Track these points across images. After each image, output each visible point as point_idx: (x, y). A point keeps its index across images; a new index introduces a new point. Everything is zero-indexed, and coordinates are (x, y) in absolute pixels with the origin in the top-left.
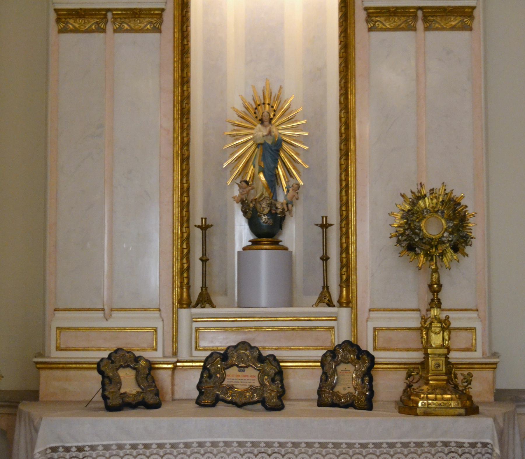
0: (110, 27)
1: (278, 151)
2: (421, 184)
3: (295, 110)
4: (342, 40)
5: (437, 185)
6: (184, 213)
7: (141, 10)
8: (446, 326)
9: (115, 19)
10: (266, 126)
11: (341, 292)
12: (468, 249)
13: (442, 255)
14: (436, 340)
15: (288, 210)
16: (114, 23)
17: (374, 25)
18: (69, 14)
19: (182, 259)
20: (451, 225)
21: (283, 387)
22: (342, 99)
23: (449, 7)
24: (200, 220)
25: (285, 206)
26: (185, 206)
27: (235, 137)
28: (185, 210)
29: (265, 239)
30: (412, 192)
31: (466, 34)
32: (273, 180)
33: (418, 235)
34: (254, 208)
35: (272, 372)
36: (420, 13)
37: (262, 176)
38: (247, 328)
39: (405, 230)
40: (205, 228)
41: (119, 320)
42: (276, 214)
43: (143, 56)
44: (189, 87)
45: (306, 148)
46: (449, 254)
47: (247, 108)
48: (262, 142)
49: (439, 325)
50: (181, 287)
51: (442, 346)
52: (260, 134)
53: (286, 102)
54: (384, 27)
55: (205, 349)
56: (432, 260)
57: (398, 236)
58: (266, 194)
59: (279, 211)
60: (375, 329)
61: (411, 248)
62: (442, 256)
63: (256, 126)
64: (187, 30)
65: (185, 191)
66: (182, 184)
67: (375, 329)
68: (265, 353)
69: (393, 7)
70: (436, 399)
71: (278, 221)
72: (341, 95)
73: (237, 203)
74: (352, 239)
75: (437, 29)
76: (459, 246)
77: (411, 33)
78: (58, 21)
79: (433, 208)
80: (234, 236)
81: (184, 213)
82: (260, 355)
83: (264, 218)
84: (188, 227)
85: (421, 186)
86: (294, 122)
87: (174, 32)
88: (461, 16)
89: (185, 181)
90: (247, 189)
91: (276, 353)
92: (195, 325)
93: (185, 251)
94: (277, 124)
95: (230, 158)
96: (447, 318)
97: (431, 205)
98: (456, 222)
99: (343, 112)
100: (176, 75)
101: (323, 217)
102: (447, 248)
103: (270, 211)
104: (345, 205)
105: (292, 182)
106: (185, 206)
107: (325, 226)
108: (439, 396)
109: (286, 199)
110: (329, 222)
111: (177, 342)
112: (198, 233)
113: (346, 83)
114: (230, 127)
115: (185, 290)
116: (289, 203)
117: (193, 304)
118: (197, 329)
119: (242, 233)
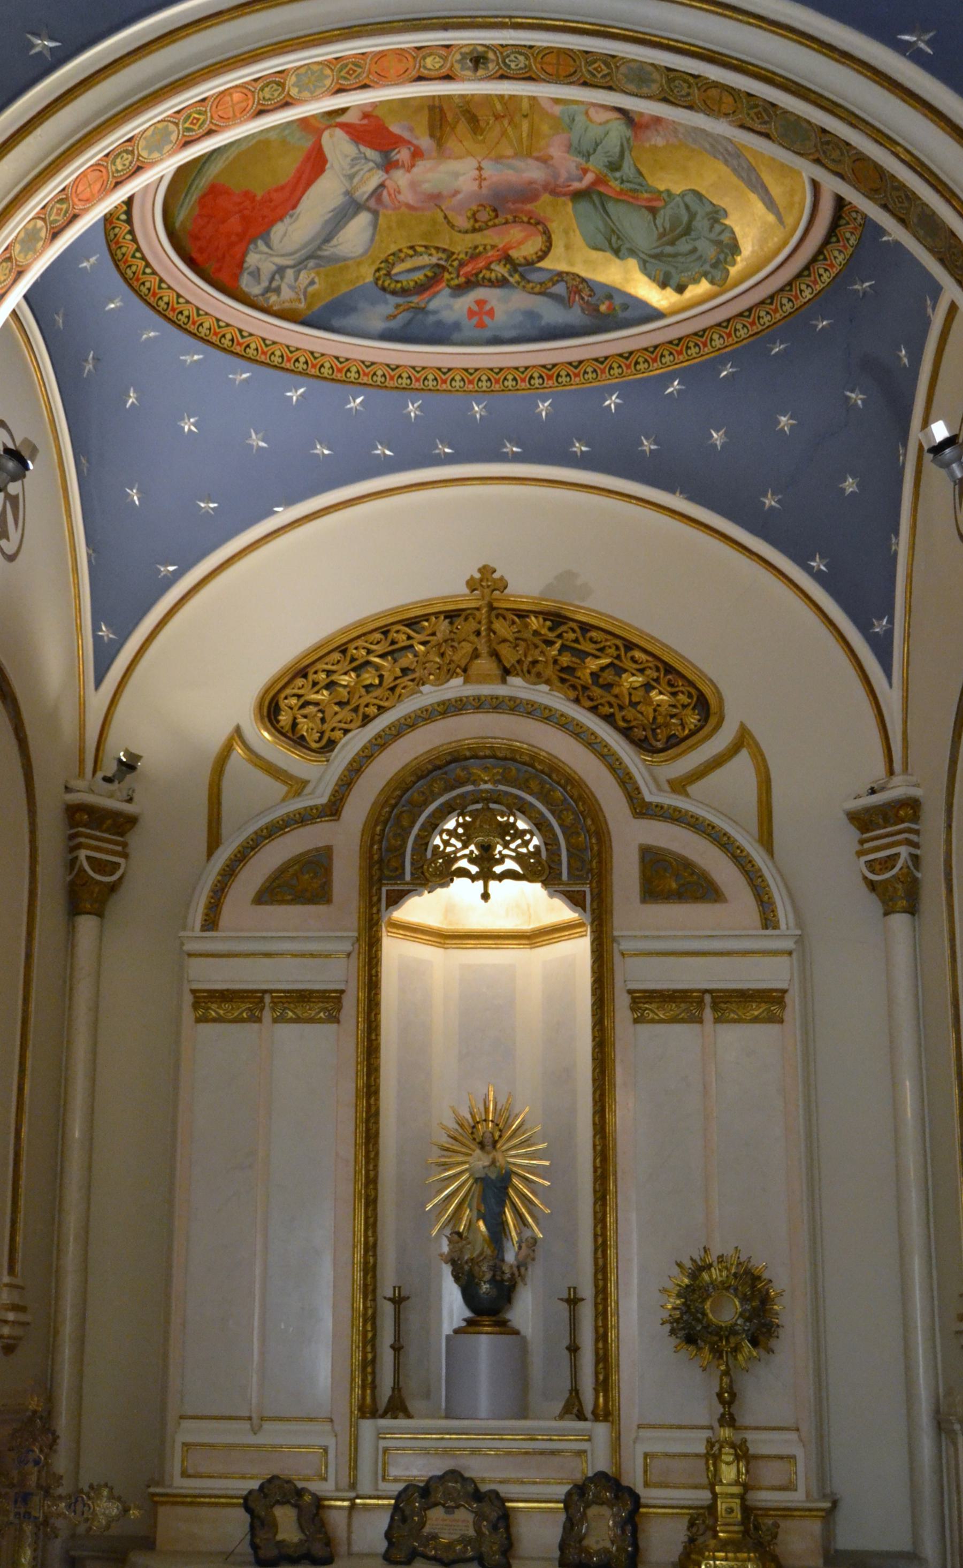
0: (267, 1015)
1: (506, 1188)
2: (705, 1248)
3: (532, 1129)
4: (596, 1034)
5: (729, 1251)
6: (369, 1279)
7: (312, 992)
8: (742, 1453)
9: (274, 1003)
10: (488, 1153)
11: (597, 1398)
12: (773, 1343)
13: (736, 1349)
14: (728, 1473)
15: (520, 1275)
16: (273, 1010)
17: (642, 1015)
18: (211, 997)
19: (364, 1347)
20: (748, 1307)
21: (509, 1537)
22: (597, 1118)
23: (749, 990)
24: (392, 1289)
25: (515, 1270)
26: (370, 1270)
27: (446, 1166)
28: (369, 1276)
29: (485, 1318)
30: (692, 1259)
31: (774, 1028)
32: (498, 1231)
33: (699, 1321)
34: (471, 1270)
35: (494, 1516)
36: (708, 998)
37: (481, 1224)
38: (459, 1449)
39: (682, 1314)
40: (398, 1301)
41: (272, 1434)
42: (502, 1281)
43: (311, 1054)
44: (377, 1100)
45: (547, 1183)
46: (746, 1350)
47: (461, 1126)
48: (483, 1176)
49: (732, 1451)
50: (364, 1388)
51: (737, 1483)
52: (480, 1164)
53: (517, 1116)
54: (656, 1017)
55: (396, 1480)
56: (721, 1357)
57: (671, 1323)
58: (488, 1252)
59: (507, 1276)
60: (646, 1455)
61: (690, 1340)
62: (736, 1351)
63: (474, 1151)
64: (376, 1020)
65: (371, 1248)
66: (366, 1237)
67: (646, 1455)
68: (484, 1488)
69: (668, 990)
70: (726, 1559)
71: (505, 1291)
72: (594, 1114)
73: (446, 1263)
74: (612, 1320)
75: (734, 1021)
76: (761, 1338)
77: (695, 1027)
78: (196, 1006)
79: (722, 1283)
80: (441, 1310)
81: (369, 1279)
82: (477, 1490)
83: (485, 1287)
84: (374, 1300)
85: (705, 1252)
86: (529, 1146)
87: (358, 1022)
88: (766, 1002)
89: (370, 1233)
90: (460, 1245)
91: (503, 1490)
92: (383, 1444)
93: (370, 1335)
94: (504, 1148)
95: (435, 1197)
96: (744, 1441)
97: (720, 1279)
98: (756, 1303)
99: (598, 1137)
100: (360, 1083)
101: (569, 1289)
102: (743, 1339)
103: (494, 1276)
104: (601, 1271)
105: (527, 1234)
106: (370, 1270)
107: (573, 1301)
108: (730, 1555)
109: (516, 1259)
110: (579, 1295)
111: (356, 1468)
112: (387, 1309)
113: (602, 1095)
114: (436, 1151)
115: (368, 1391)
116: (521, 1265)
117: (381, 1412)
118: (386, 1450)
119: (452, 1305)
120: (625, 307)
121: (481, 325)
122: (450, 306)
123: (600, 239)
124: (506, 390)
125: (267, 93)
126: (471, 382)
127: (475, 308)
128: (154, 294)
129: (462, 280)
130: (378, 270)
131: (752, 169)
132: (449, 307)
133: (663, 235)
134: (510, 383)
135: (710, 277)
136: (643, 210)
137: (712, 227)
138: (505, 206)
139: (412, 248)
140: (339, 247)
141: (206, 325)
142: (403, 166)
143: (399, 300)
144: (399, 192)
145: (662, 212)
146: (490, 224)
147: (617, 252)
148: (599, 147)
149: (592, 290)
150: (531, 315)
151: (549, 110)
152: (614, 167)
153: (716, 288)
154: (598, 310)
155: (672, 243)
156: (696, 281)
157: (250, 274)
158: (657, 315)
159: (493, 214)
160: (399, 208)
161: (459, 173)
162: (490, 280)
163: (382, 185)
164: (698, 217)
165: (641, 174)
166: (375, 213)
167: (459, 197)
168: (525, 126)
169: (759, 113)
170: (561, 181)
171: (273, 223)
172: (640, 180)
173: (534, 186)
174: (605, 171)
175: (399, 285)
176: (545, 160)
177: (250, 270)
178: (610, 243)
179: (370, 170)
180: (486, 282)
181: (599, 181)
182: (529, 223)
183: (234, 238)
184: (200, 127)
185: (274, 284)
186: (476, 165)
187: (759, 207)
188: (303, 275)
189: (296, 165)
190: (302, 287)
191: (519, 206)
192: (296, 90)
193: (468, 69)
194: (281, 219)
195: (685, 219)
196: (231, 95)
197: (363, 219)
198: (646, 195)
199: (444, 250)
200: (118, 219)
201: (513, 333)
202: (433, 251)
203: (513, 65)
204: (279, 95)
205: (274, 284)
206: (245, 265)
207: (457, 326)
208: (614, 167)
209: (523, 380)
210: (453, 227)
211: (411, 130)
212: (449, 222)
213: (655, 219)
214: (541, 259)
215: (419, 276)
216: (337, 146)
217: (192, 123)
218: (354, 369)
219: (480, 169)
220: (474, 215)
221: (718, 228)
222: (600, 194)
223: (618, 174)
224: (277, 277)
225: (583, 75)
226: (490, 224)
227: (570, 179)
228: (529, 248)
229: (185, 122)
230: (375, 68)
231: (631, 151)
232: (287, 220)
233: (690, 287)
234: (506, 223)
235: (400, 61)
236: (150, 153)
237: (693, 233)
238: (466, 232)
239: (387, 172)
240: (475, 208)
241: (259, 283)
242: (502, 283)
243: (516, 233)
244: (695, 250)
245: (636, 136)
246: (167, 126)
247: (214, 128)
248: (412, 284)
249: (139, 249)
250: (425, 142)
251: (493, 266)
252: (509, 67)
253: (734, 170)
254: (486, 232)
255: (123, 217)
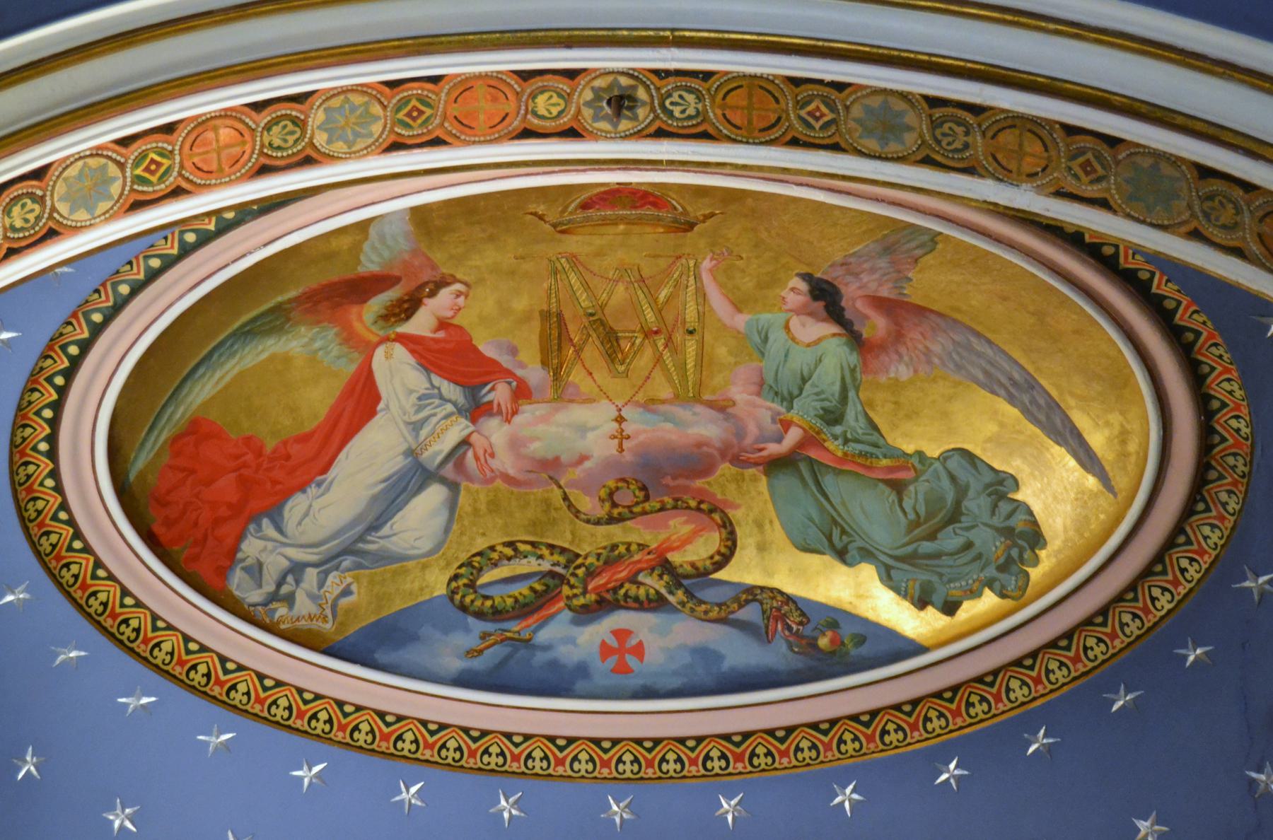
120: (860, 640)
121: (622, 669)
122: (571, 639)
123: (814, 535)
124: (664, 777)
125: (275, 136)
126: (605, 764)
127: (613, 642)
128: (84, 587)
129: (592, 597)
130: (456, 577)
131: (1053, 405)
132: (572, 641)
133: (916, 524)
134: (671, 767)
135: (997, 585)
136: (881, 486)
137: (995, 507)
138: (660, 480)
139: (510, 544)
140: (394, 539)
141: (166, 647)
142: (500, 412)
143: (489, 627)
144: (492, 455)
145: (911, 488)
146: (637, 509)
147: (842, 555)
148: (807, 386)
149: (803, 614)
150: (704, 654)
151: (727, 321)
152: (833, 417)
153: (1008, 603)
154: (813, 644)
155: (932, 536)
156: (975, 594)
157: (245, 569)
158: (916, 649)
159: (641, 495)
160: (492, 480)
161: (586, 427)
162: (636, 599)
163: (465, 443)
164: (971, 493)
165: (875, 427)
166: (454, 487)
167: (588, 464)
168: (691, 347)
169: (1088, 162)
170: (748, 441)
171: (288, 494)
172: (875, 437)
173: (705, 449)
174: (819, 424)
175: (489, 603)
176: (722, 407)
177: (249, 562)
178: (829, 538)
179: (447, 417)
180: (631, 603)
181: (810, 440)
182: (698, 509)
183: (224, 512)
184: (161, 179)
185: (285, 589)
186: (615, 414)
187: (1065, 463)
188: (333, 578)
189: (331, 401)
190: (330, 597)
191: (681, 482)
192: (325, 136)
193: (605, 118)
194: (302, 488)
195: (950, 497)
196: (215, 129)
197: (434, 495)
198: (885, 462)
199: (563, 551)
200: (35, 449)
201: (675, 683)
202: (546, 552)
203: (677, 111)
204: (296, 141)
205: (285, 589)
206: (240, 555)
207: (582, 670)
208: (833, 417)
209: (693, 762)
210: (577, 513)
211: (513, 351)
212: (570, 506)
213: (900, 501)
214: (719, 566)
215: (522, 590)
216: (397, 372)
217: (147, 169)
218: (409, 737)
219: (620, 420)
220: (611, 494)
221: (1004, 508)
222: (811, 462)
223: (838, 430)
224: (290, 579)
225: (790, 127)
226: (637, 509)
227: (763, 438)
228: (702, 549)
229: (137, 164)
230: (455, 110)
231: (857, 390)
232: (312, 490)
233: (966, 605)
234: (662, 509)
235: (495, 99)
236: (72, 210)
237: (963, 519)
238: (598, 522)
239: (474, 420)
240: (612, 484)
241: (260, 586)
242: (656, 604)
243: (679, 526)
244: (969, 545)
245: (865, 364)
246: (105, 166)
247: (184, 185)
248: (510, 601)
249: (64, 506)
250: (534, 374)
251: (641, 578)
252: (670, 114)
253: (1026, 412)
254: (628, 523)
255: (43, 446)
